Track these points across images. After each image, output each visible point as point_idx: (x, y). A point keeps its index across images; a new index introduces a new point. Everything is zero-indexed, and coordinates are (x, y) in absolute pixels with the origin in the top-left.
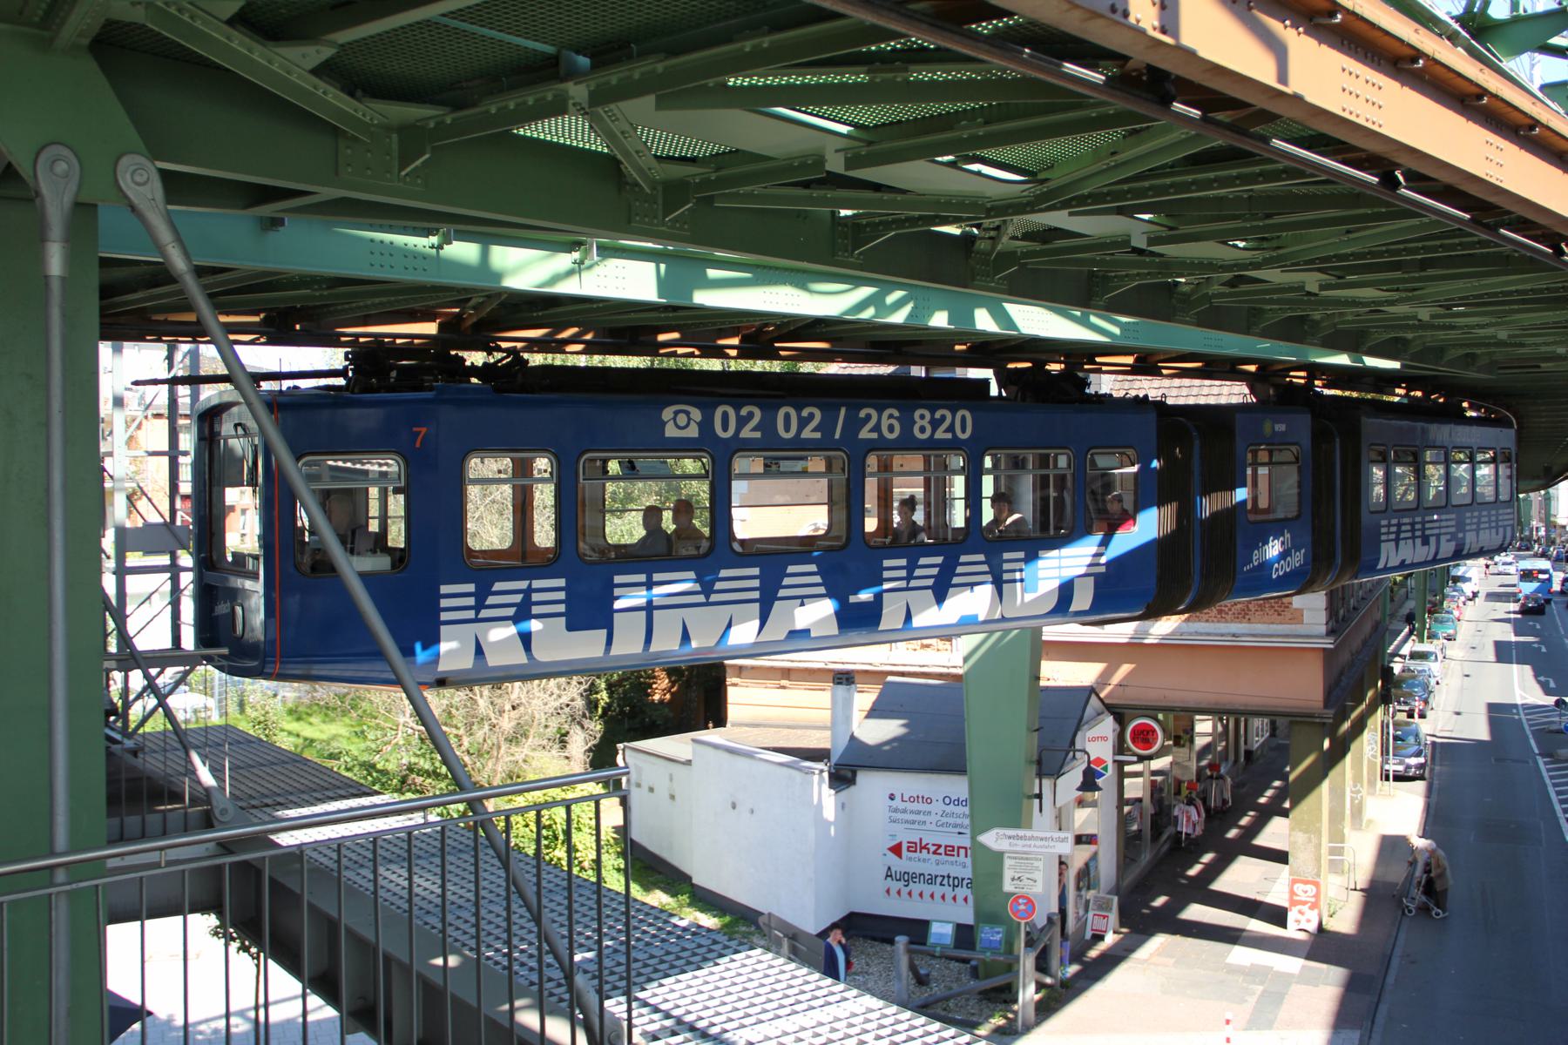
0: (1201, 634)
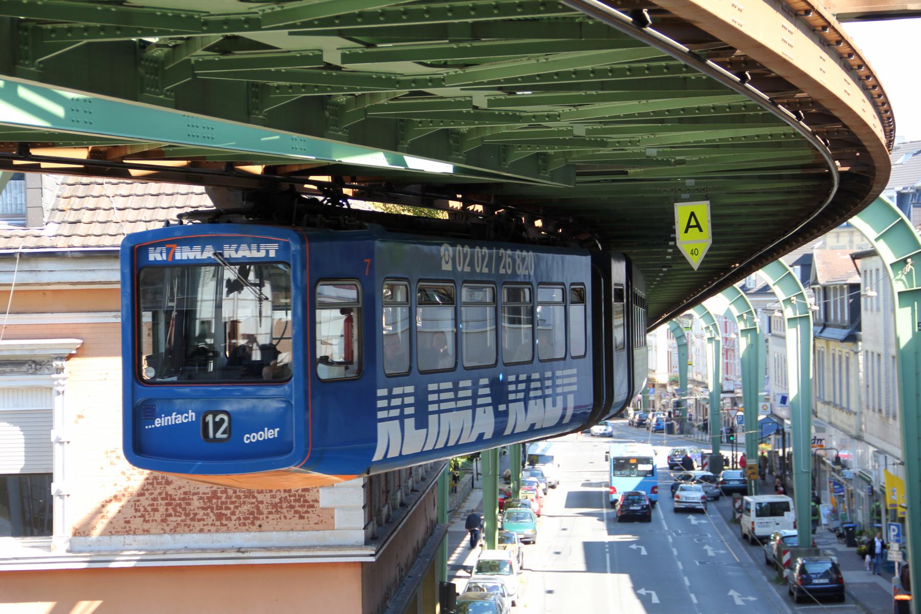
0: (193, 550)
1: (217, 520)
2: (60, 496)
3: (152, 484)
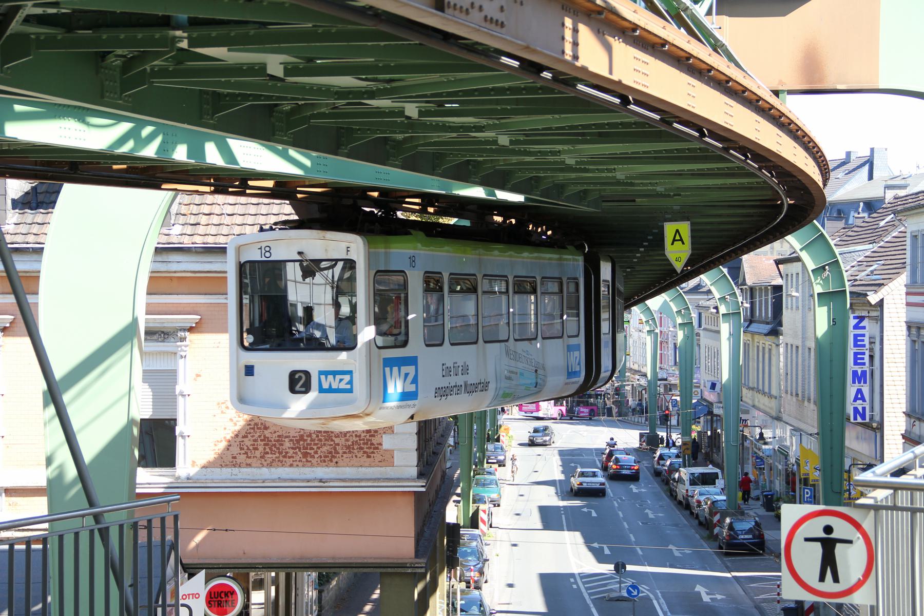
0: (285, 480)
1: (303, 458)
2: (182, 436)
3: (253, 429)
